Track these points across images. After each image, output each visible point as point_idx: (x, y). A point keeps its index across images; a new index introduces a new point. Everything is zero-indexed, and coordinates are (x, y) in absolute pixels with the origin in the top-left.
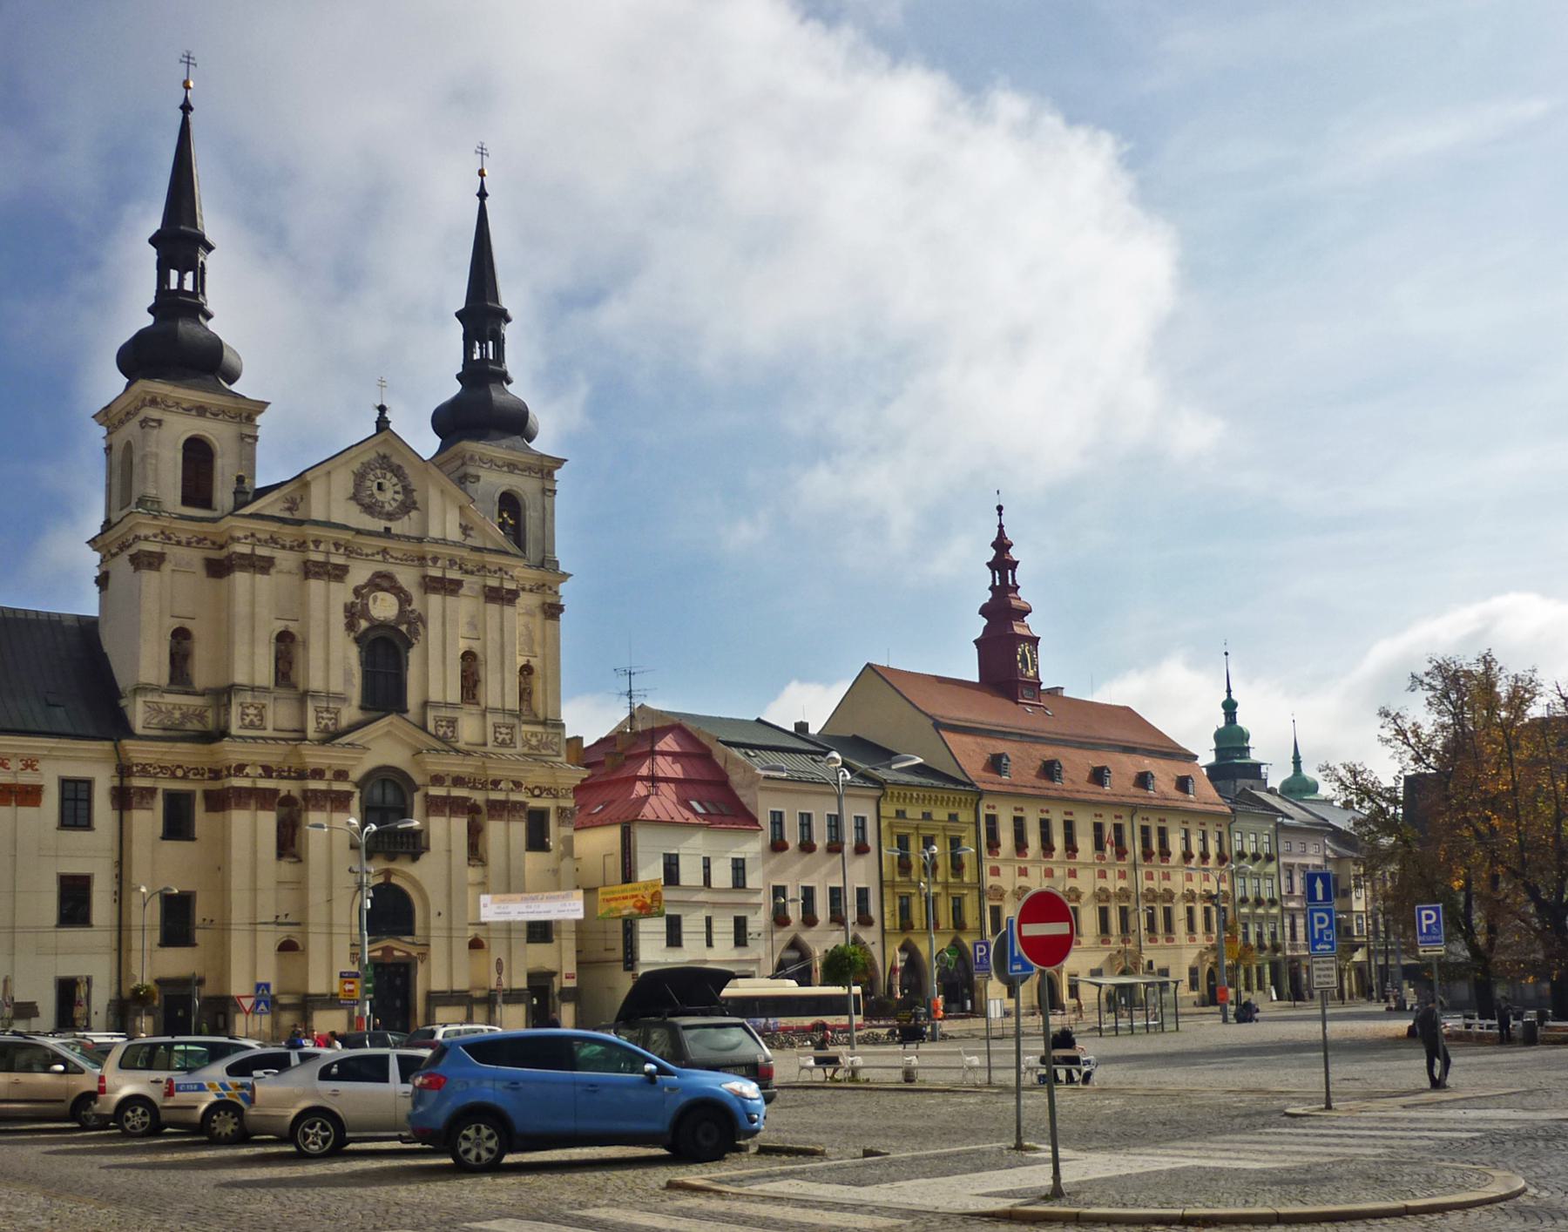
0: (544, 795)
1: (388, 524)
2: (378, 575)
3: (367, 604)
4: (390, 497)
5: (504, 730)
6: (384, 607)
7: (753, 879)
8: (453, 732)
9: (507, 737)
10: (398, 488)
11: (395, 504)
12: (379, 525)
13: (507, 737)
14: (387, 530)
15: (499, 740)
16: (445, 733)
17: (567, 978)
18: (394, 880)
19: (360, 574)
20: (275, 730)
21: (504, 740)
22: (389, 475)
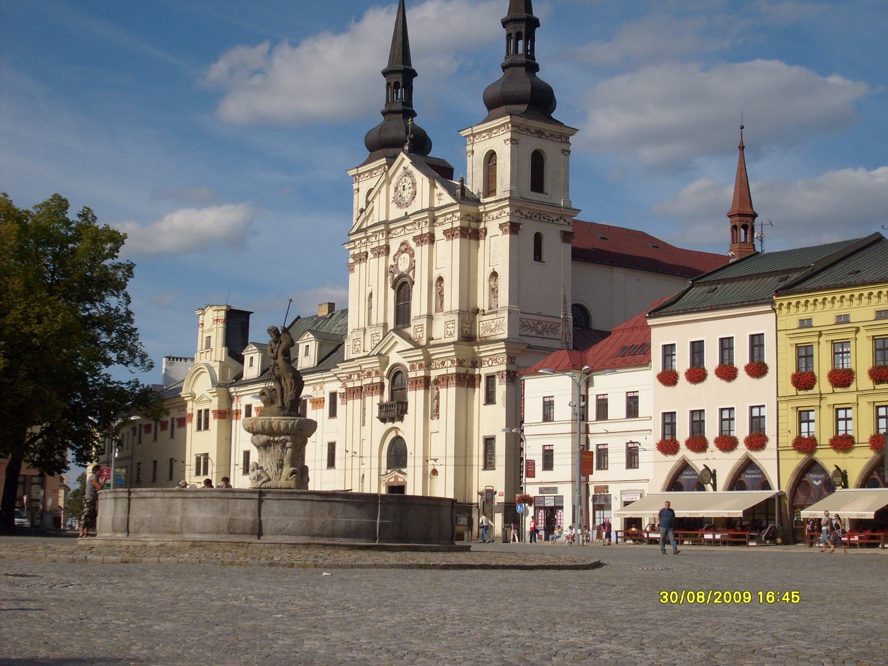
0: (494, 364)
1: (406, 210)
2: (402, 244)
3: (397, 264)
4: (407, 194)
5: (451, 326)
6: (403, 267)
7: (644, 408)
8: (423, 334)
9: (452, 330)
10: (411, 185)
11: (409, 196)
12: (400, 213)
13: (452, 330)
14: (406, 213)
15: (449, 333)
16: (420, 336)
17: (500, 495)
18: (400, 434)
19: (395, 246)
20: (364, 351)
21: (451, 332)
22: (407, 178)
